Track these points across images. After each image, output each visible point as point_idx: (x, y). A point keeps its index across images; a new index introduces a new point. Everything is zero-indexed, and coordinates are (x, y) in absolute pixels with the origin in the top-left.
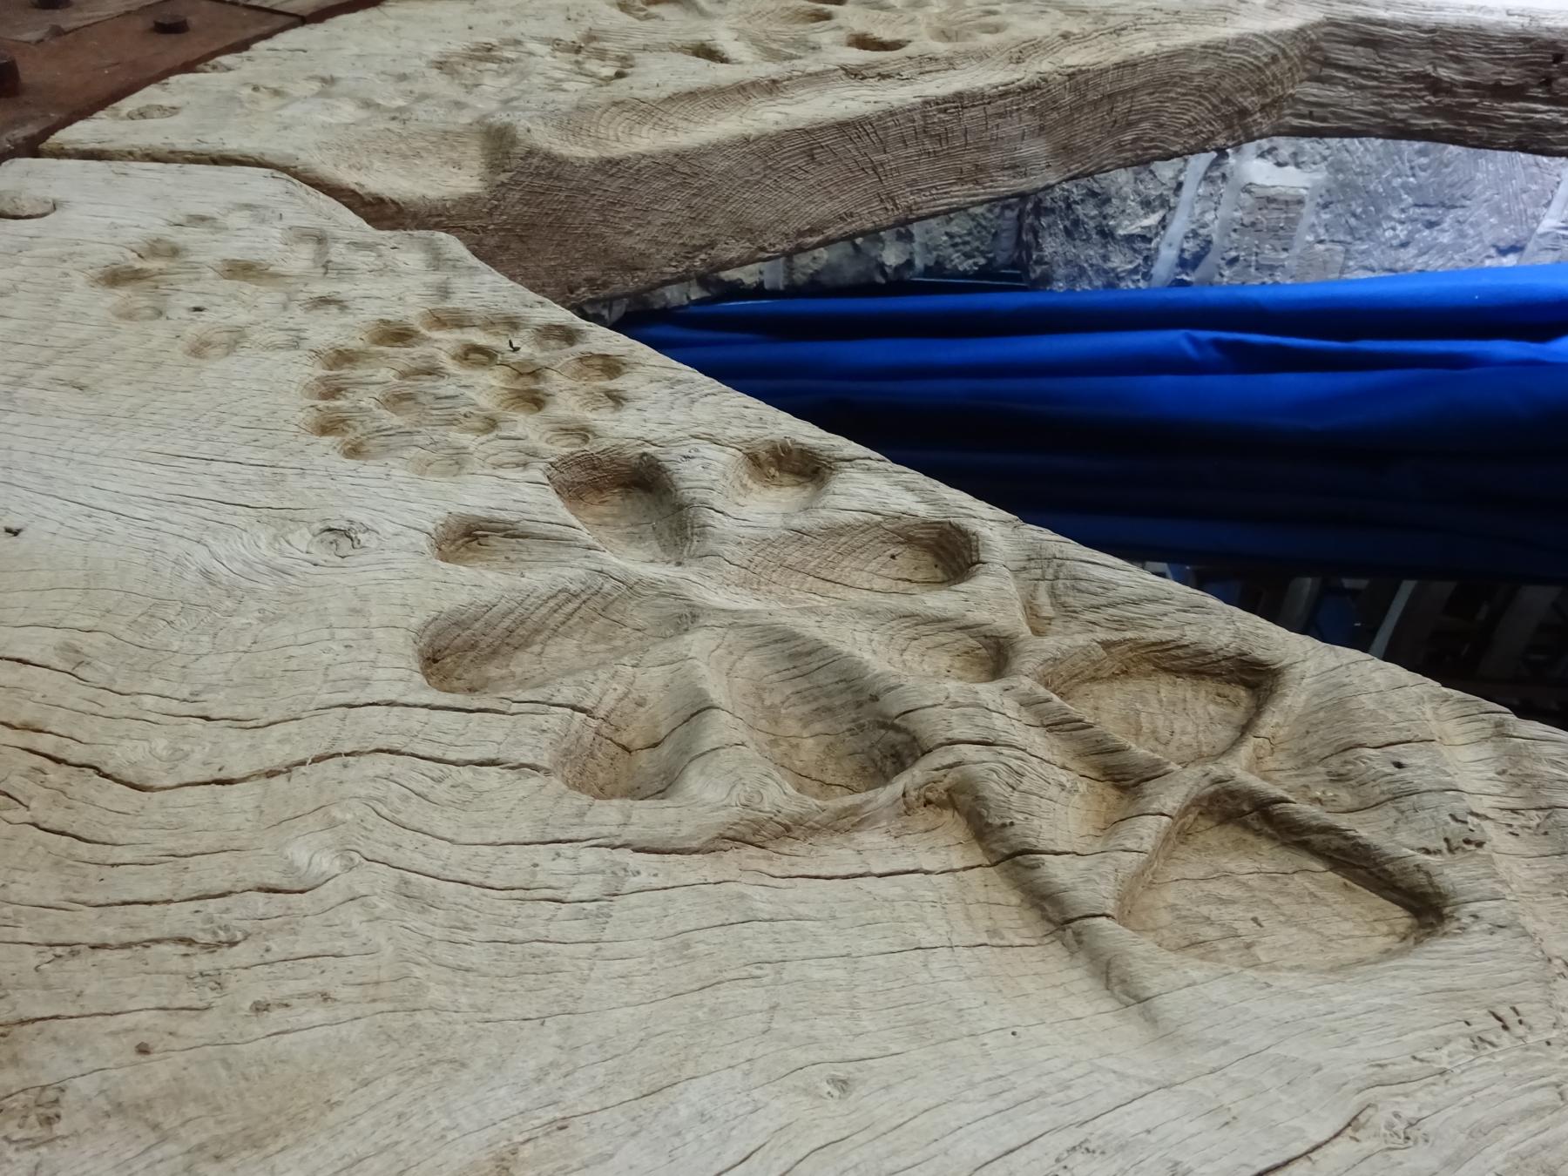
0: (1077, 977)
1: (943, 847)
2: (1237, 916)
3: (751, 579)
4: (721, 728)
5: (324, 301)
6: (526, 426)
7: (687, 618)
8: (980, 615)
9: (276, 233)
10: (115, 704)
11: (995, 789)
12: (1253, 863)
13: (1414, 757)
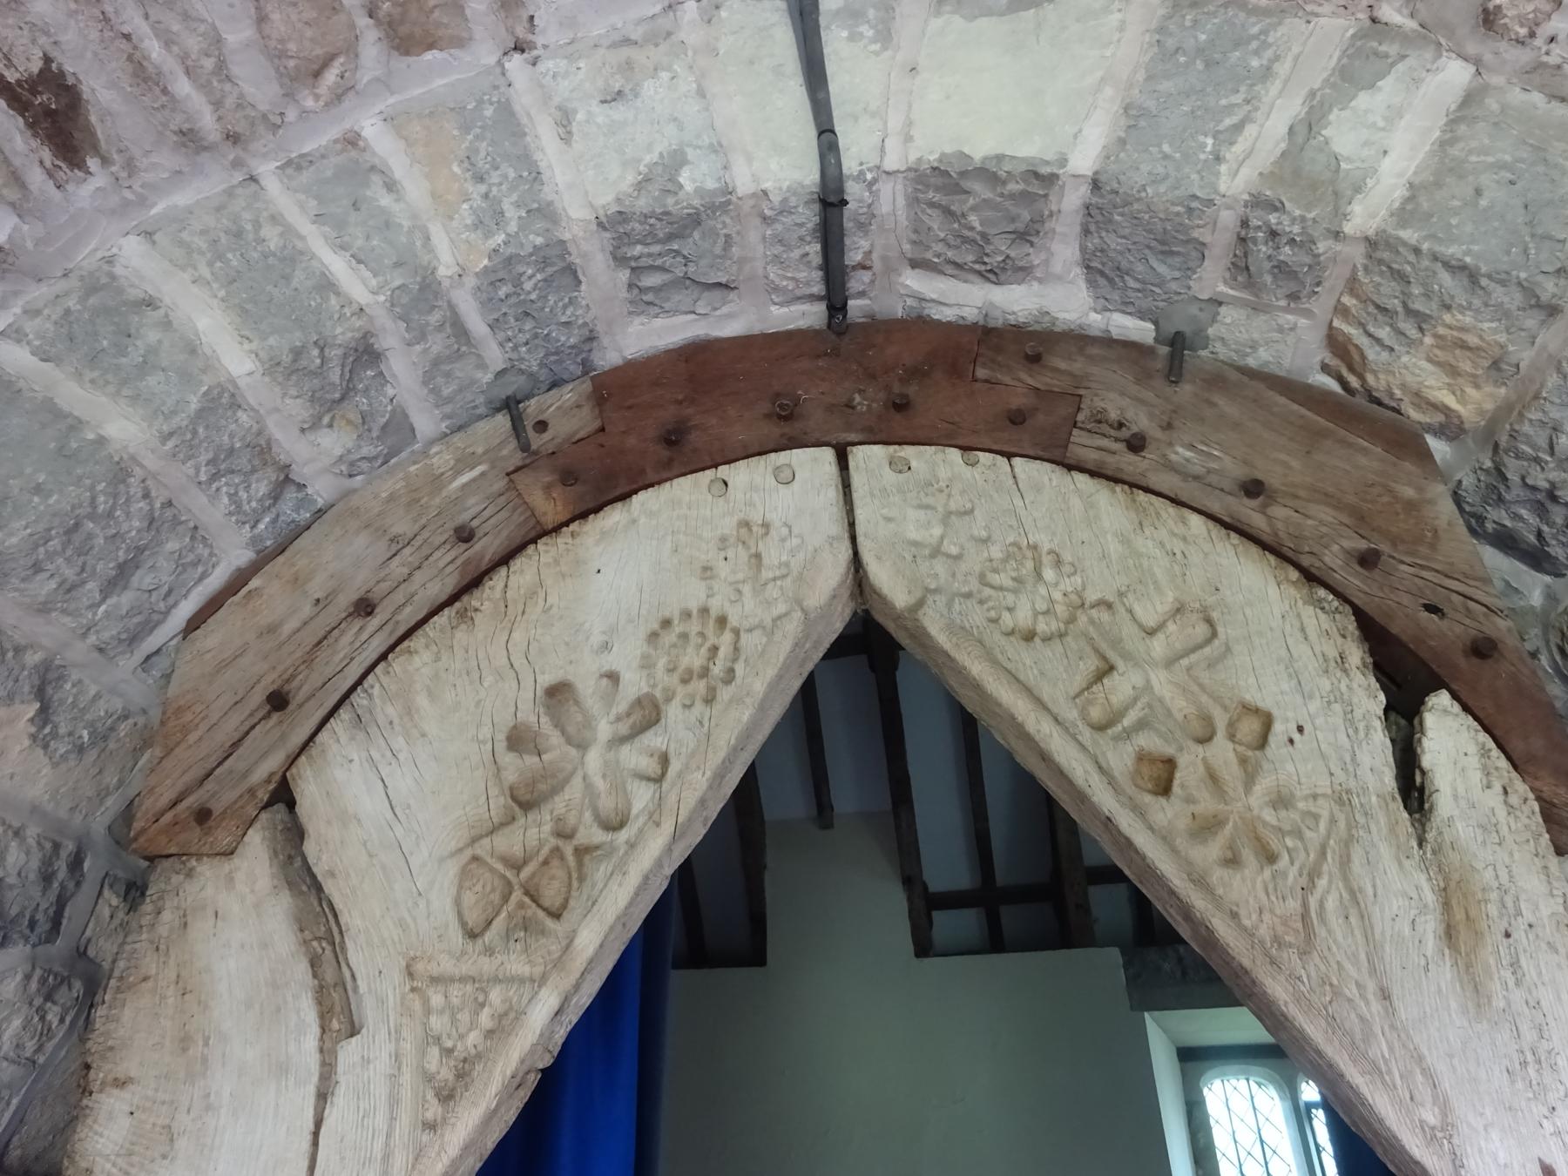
0: (461, 845)
1: (496, 816)
2: (478, 888)
3: (606, 763)
4: (531, 760)
5: (739, 592)
6: (675, 679)
7: (583, 746)
9: (784, 558)
12: (496, 897)
13: (518, 946)
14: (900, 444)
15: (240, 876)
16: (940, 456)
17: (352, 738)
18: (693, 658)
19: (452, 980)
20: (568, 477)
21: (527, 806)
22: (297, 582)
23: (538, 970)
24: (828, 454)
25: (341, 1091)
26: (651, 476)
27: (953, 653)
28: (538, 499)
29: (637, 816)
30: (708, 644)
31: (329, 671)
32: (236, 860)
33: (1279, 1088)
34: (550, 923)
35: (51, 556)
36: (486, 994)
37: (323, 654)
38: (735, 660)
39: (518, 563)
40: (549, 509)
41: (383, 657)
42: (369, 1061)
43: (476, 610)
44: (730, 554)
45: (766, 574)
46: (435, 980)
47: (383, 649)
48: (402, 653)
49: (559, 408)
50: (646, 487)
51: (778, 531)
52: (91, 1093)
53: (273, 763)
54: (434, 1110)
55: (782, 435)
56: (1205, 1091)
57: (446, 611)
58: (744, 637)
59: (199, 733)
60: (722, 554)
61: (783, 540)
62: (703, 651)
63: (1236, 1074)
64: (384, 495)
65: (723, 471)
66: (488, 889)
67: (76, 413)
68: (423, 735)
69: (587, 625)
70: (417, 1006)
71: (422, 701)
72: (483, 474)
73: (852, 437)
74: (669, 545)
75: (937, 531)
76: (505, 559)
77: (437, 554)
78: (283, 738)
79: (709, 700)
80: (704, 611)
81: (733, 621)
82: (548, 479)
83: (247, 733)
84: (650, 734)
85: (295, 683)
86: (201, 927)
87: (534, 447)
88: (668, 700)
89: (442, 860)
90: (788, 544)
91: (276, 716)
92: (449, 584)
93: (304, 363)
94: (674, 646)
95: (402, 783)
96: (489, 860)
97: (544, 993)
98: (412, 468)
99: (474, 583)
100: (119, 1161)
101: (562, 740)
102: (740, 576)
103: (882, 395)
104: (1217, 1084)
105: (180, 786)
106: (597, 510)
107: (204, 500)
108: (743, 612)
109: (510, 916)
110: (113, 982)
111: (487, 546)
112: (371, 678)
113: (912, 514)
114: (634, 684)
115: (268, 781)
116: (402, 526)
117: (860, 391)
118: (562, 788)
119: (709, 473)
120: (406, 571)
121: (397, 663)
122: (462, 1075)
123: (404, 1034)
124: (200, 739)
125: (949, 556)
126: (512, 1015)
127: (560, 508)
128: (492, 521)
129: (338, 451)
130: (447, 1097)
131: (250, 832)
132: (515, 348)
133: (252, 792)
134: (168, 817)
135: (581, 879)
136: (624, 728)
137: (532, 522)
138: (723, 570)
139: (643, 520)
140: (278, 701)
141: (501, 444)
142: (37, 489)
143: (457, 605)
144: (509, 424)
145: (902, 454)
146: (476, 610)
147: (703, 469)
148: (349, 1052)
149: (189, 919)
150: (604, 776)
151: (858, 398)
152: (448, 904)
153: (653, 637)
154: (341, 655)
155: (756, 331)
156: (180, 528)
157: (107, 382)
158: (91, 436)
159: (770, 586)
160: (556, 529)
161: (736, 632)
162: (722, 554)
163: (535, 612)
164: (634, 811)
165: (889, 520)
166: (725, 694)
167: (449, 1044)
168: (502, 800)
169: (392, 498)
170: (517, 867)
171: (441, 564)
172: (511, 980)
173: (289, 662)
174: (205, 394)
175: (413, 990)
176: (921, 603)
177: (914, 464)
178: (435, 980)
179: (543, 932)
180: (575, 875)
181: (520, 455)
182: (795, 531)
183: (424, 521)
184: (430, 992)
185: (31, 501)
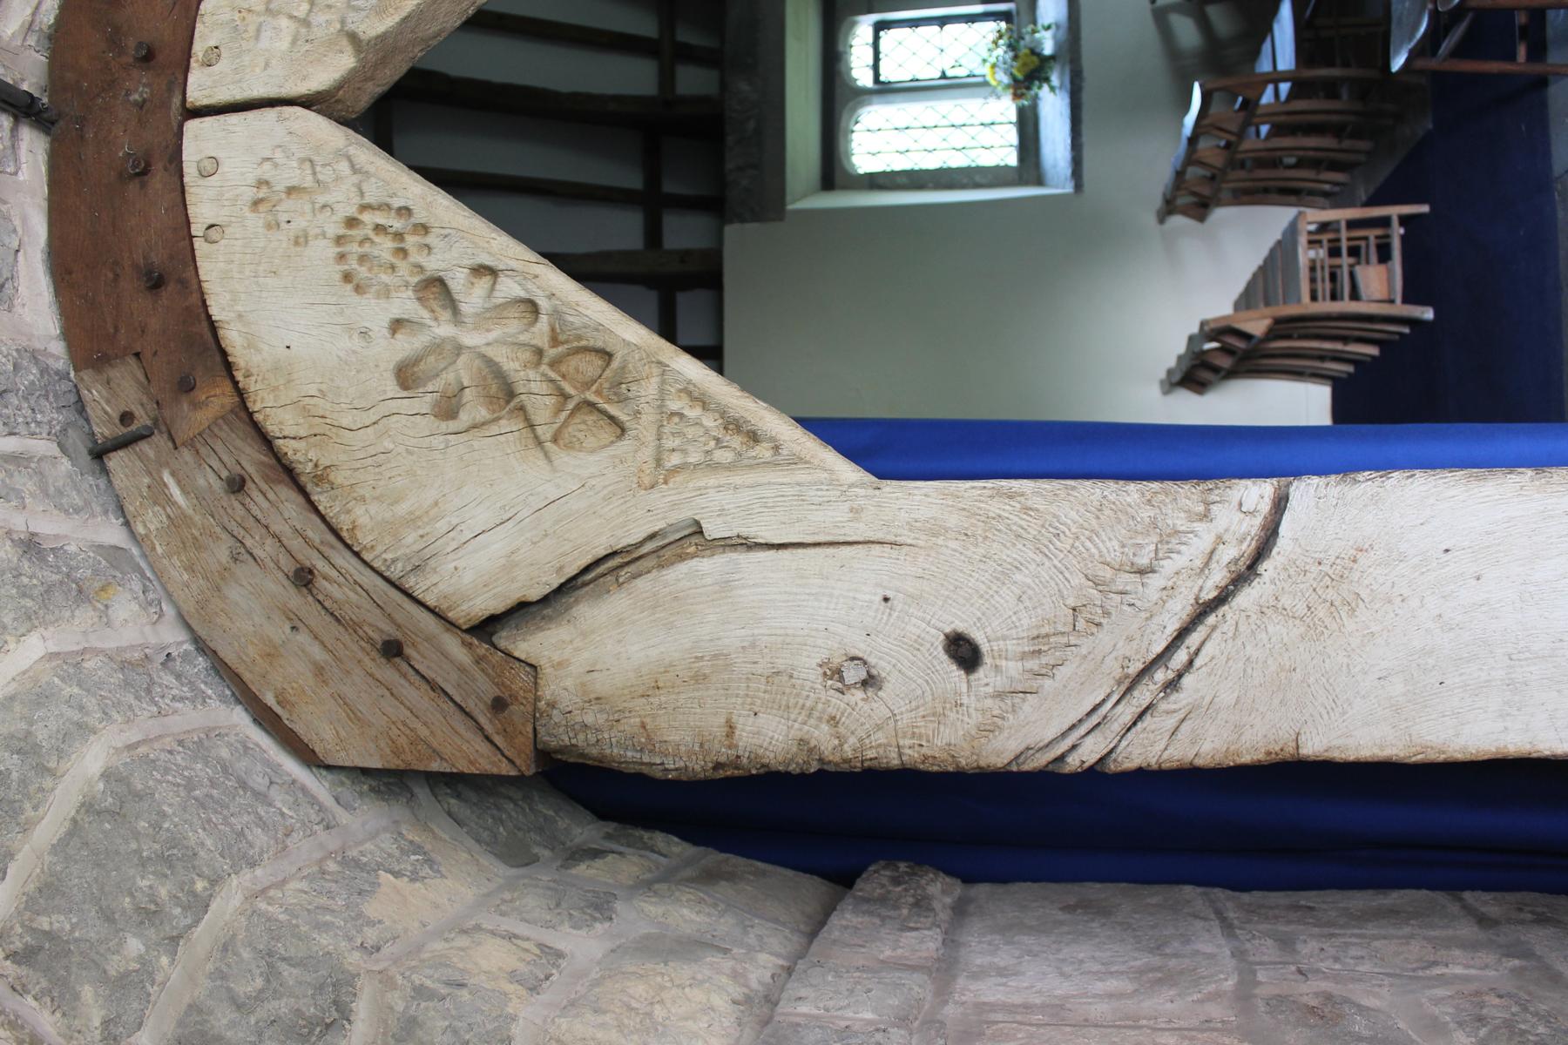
0: (541, 455)
2: (581, 435)
3: (476, 328)
5: (324, 206)
6: (403, 267)
7: (459, 349)
8: (534, 342)
9: (295, 164)
10: (337, 408)
11: (529, 408)
12: (591, 418)
13: (634, 387)
14: (190, 57)
15: (556, 658)
16: (206, 19)
17: (434, 570)
18: (385, 245)
19: (660, 446)
20: (186, 386)
21: (510, 394)
22: (272, 654)
23: (656, 370)
24: (191, 126)
25: (744, 532)
26: (194, 299)
27: (404, 14)
28: (203, 417)
29: (527, 290)
30: (371, 234)
31: (366, 603)
32: (543, 662)
33: (862, 104)
34: (615, 364)
35: (226, 822)
36: (673, 414)
37: (348, 613)
38: (388, 206)
39: (272, 428)
40: (219, 399)
41: (357, 555)
42: (721, 504)
43: (316, 466)
44: (284, 217)
45: (308, 182)
46: (659, 462)
47: (348, 554)
48: (354, 537)
49: (108, 402)
50: (205, 306)
51: (267, 171)
52: (738, 757)
53: (453, 645)
54: (763, 451)
55: (166, 169)
56: (861, 171)
57: (314, 498)
58: (368, 200)
59: (418, 726)
60: (284, 226)
61: (276, 165)
62: (377, 239)
63: (849, 142)
64: (186, 577)
65: (197, 230)
66: (583, 427)
67: (73, 813)
68: (436, 504)
69: (342, 354)
70: (679, 478)
71: (402, 509)
72: (173, 474)
73: (177, 101)
74: (268, 280)
75: (284, 22)
76: (265, 440)
77: (255, 511)
78: (429, 639)
79: (424, 229)
80: (339, 240)
81: (352, 211)
82: (185, 406)
83: (423, 677)
84: (452, 285)
85: (375, 636)
86: (601, 685)
87: (149, 423)
88: (420, 268)
89: (554, 470)
90: (280, 161)
91: (408, 651)
92: (287, 493)
93: (36, 592)
94: (370, 270)
95: (481, 517)
96: (556, 426)
97: (674, 365)
98: (159, 550)
99: (288, 473)
100: (793, 717)
101: (451, 369)
102: (307, 208)
103: (135, 73)
104: (856, 160)
105: (469, 735)
106: (224, 354)
107: (176, 717)
108: (344, 200)
109: (609, 401)
110: (646, 759)
111: (250, 458)
112: (375, 565)
113: (264, 43)
114: (405, 304)
115: (469, 646)
116: (223, 555)
117: (127, 95)
118: (496, 364)
119: (198, 243)
120: (269, 541)
121: (364, 539)
122: (734, 425)
123: (702, 484)
124: (425, 724)
125: (310, 11)
126: (691, 388)
127: (218, 391)
128: (225, 458)
129: (135, 607)
130: (754, 437)
131: (516, 654)
132: (38, 423)
133: (478, 660)
134: (498, 740)
135: (579, 338)
136: (446, 315)
137: (231, 417)
138: (300, 223)
139: (239, 308)
140: (392, 650)
141: (142, 457)
142: (157, 826)
143: (309, 487)
144: (121, 453)
145: (200, 55)
146: (316, 466)
147: (193, 250)
148: (713, 529)
149: (592, 696)
150: (488, 330)
151: (136, 97)
152: (592, 458)
153: (358, 289)
154: (351, 594)
155: (45, 204)
156: (206, 743)
157: (41, 789)
158: (101, 786)
159: (321, 177)
160: (241, 393)
161: (365, 208)
162: (284, 226)
163: (322, 405)
164: (523, 294)
165: (267, 65)
166: (420, 216)
167: (713, 443)
168: (503, 422)
169: (190, 568)
170: (566, 397)
171: (265, 505)
172: (662, 391)
173: (355, 647)
174: (63, 679)
175: (666, 482)
176: (353, 38)
177: (213, 43)
178: (659, 462)
179: (623, 368)
180: (575, 344)
181: (156, 438)
182: (268, 154)
183: (218, 530)
184: (668, 465)
185: (168, 830)
